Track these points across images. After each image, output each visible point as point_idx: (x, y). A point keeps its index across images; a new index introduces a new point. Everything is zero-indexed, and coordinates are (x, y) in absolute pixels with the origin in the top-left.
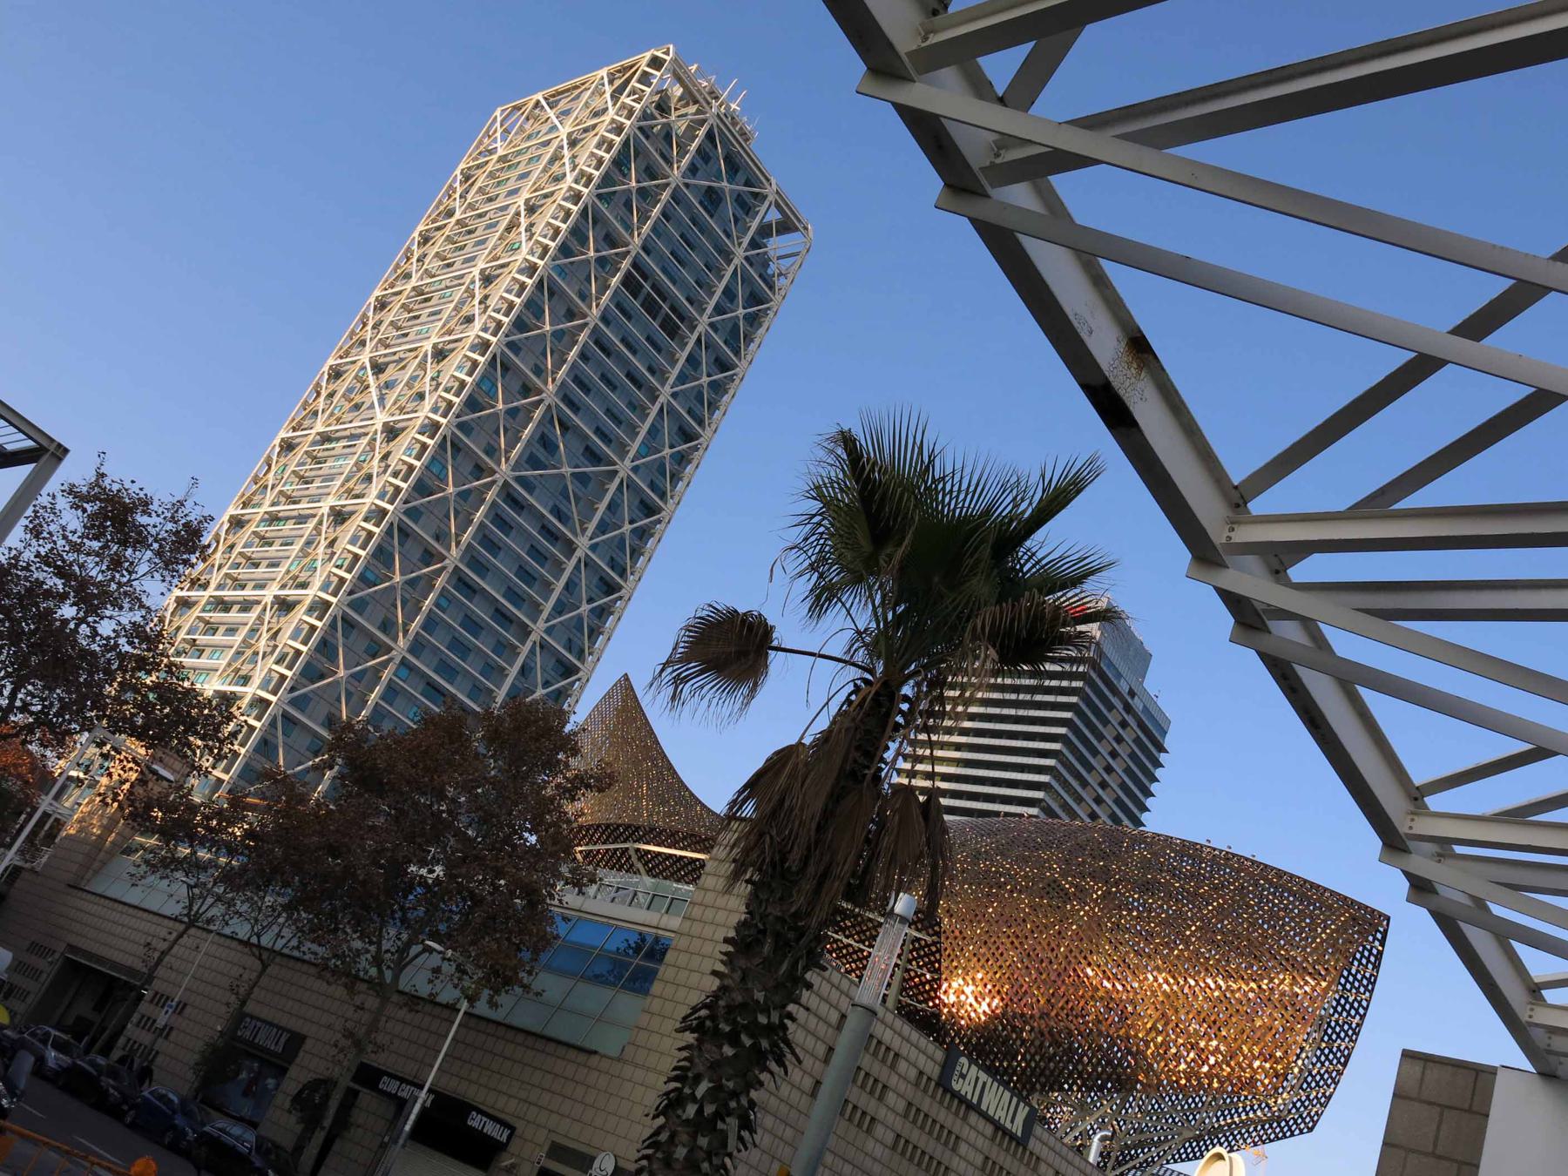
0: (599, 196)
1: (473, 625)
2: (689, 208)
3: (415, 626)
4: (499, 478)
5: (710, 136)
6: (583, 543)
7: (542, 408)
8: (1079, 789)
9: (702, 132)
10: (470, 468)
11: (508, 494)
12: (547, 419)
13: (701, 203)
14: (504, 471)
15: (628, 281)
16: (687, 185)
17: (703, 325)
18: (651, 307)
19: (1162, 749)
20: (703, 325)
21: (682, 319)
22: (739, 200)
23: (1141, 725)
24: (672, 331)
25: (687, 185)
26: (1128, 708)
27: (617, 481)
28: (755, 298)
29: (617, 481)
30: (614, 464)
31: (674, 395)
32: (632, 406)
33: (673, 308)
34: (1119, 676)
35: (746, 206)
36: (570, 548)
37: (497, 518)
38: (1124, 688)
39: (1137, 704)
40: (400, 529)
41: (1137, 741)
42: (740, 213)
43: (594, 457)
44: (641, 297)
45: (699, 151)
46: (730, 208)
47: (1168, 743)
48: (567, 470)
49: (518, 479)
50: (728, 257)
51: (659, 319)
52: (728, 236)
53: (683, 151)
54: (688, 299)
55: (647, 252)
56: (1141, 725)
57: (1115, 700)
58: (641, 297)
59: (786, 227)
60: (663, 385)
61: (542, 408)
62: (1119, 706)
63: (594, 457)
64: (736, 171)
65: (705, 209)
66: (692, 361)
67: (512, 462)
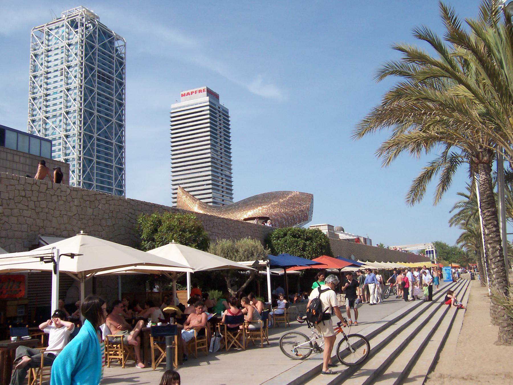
1: (102, 170)
3: (95, 177)
4: (95, 137)
5: (99, 30)
6: (114, 141)
9: (97, 30)
11: (98, 140)
14: (95, 136)
15: (99, 77)
18: (103, 80)
19: (228, 117)
23: (223, 114)
24: (109, 82)
26: (219, 112)
28: (121, 64)
32: (109, 105)
34: (215, 105)
35: (111, 42)
36: (111, 144)
37: (98, 146)
38: (217, 107)
39: (221, 110)
43: (108, 121)
47: (230, 115)
56: (223, 114)
63: (108, 121)
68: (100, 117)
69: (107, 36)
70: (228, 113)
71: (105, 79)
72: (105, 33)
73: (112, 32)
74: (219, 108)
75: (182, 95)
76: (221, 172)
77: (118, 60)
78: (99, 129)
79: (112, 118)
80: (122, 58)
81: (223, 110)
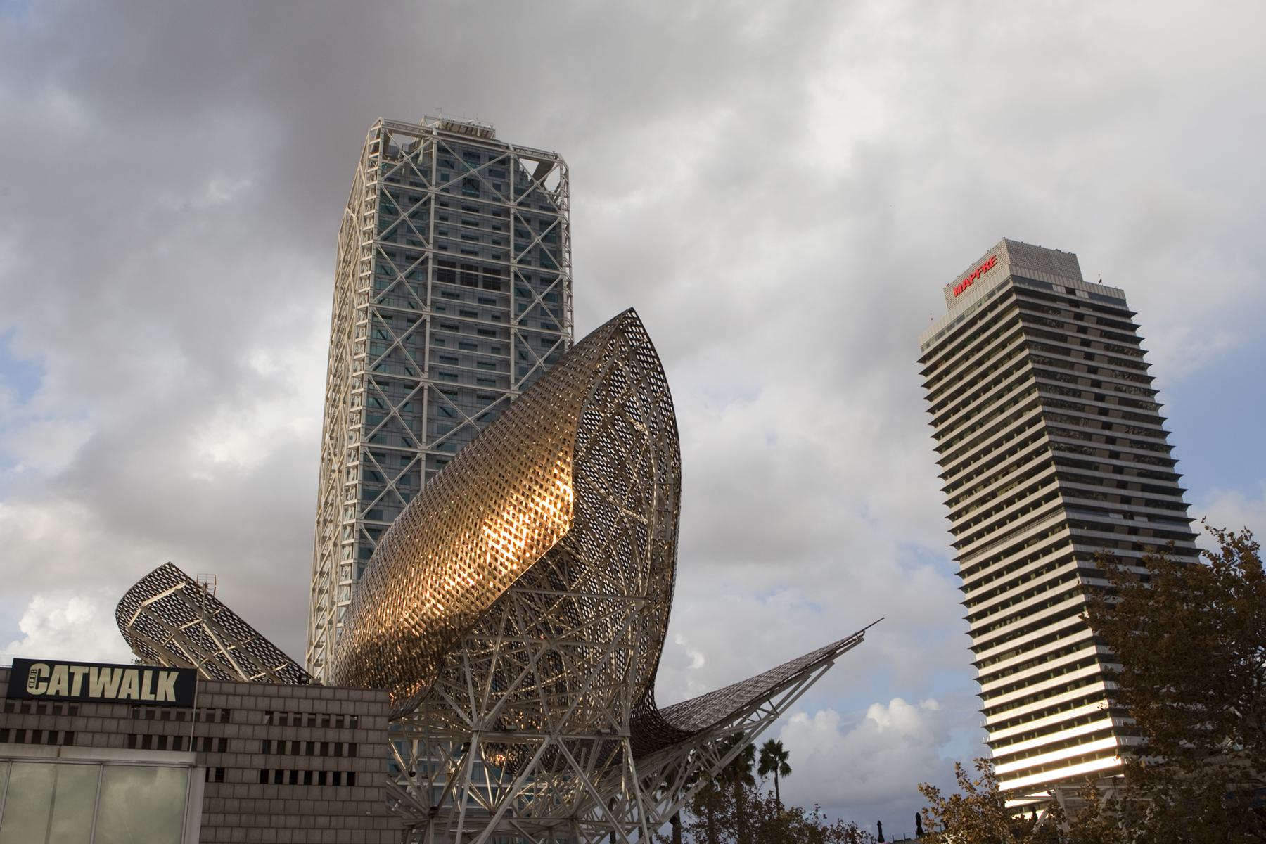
0: (385, 239)
2: (458, 203)
5: (441, 149)
7: (426, 392)
8: (1072, 386)
9: (434, 149)
10: (399, 461)
13: (464, 194)
14: (423, 449)
15: (441, 276)
16: (443, 190)
17: (514, 265)
18: (469, 281)
20: (514, 265)
21: (497, 272)
22: (491, 172)
24: (496, 285)
25: (443, 190)
26: (1076, 304)
31: (521, 323)
32: (496, 350)
33: (486, 270)
34: (1049, 286)
38: (1059, 291)
39: (1082, 296)
40: (368, 530)
41: (1100, 321)
42: (497, 180)
44: (458, 277)
45: (439, 163)
46: (487, 184)
48: (470, 420)
49: (439, 446)
50: (506, 212)
51: (481, 284)
52: (498, 200)
53: (426, 172)
54: (495, 257)
55: (443, 248)
57: (1057, 305)
59: (545, 167)
61: (426, 392)
62: (1066, 306)
65: (473, 196)
66: (521, 292)
70: (1123, 302)
76: (1126, 507)
81: (1091, 295)
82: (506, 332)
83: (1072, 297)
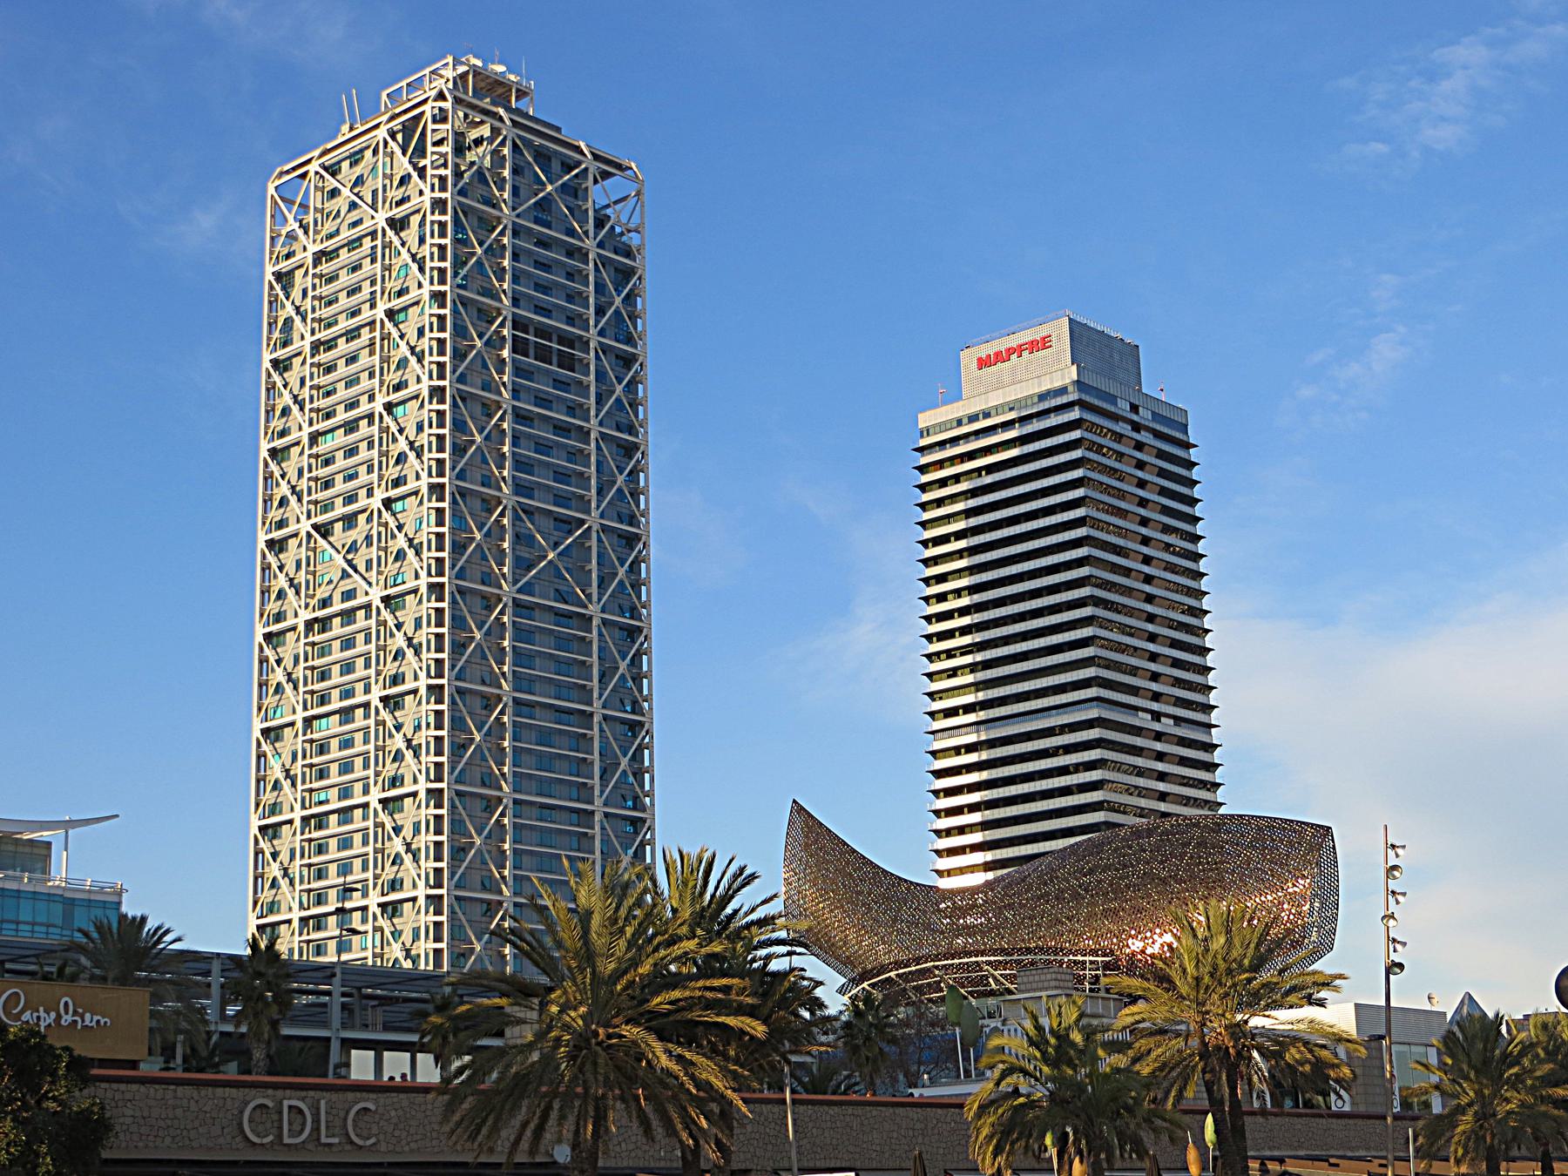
6: (593, 609)
12: (516, 518)
15: (519, 347)
18: (543, 354)
19: (1188, 446)
24: (568, 362)
27: (594, 535)
28: (625, 274)
29: (594, 535)
30: (583, 522)
34: (1112, 399)
35: (573, 191)
38: (1123, 407)
39: (1144, 416)
43: (569, 525)
44: (532, 352)
58: (532, 352)
60: (588, 421)
63: (569, 525)
64: (549, 159)
67: (510, 579)
68: (529, 512)
69: (556, 166)
70: (1184, 428)
71: (547, 349)
72: (542, 157)
73: (578, 150)
74: (1134, 408)
75: (980, 359)
77: (605, 261)
78: (523, 565)
79: (588, 512)
80: (628, 253)
82: (584, 435)
83: (1135, 418)
